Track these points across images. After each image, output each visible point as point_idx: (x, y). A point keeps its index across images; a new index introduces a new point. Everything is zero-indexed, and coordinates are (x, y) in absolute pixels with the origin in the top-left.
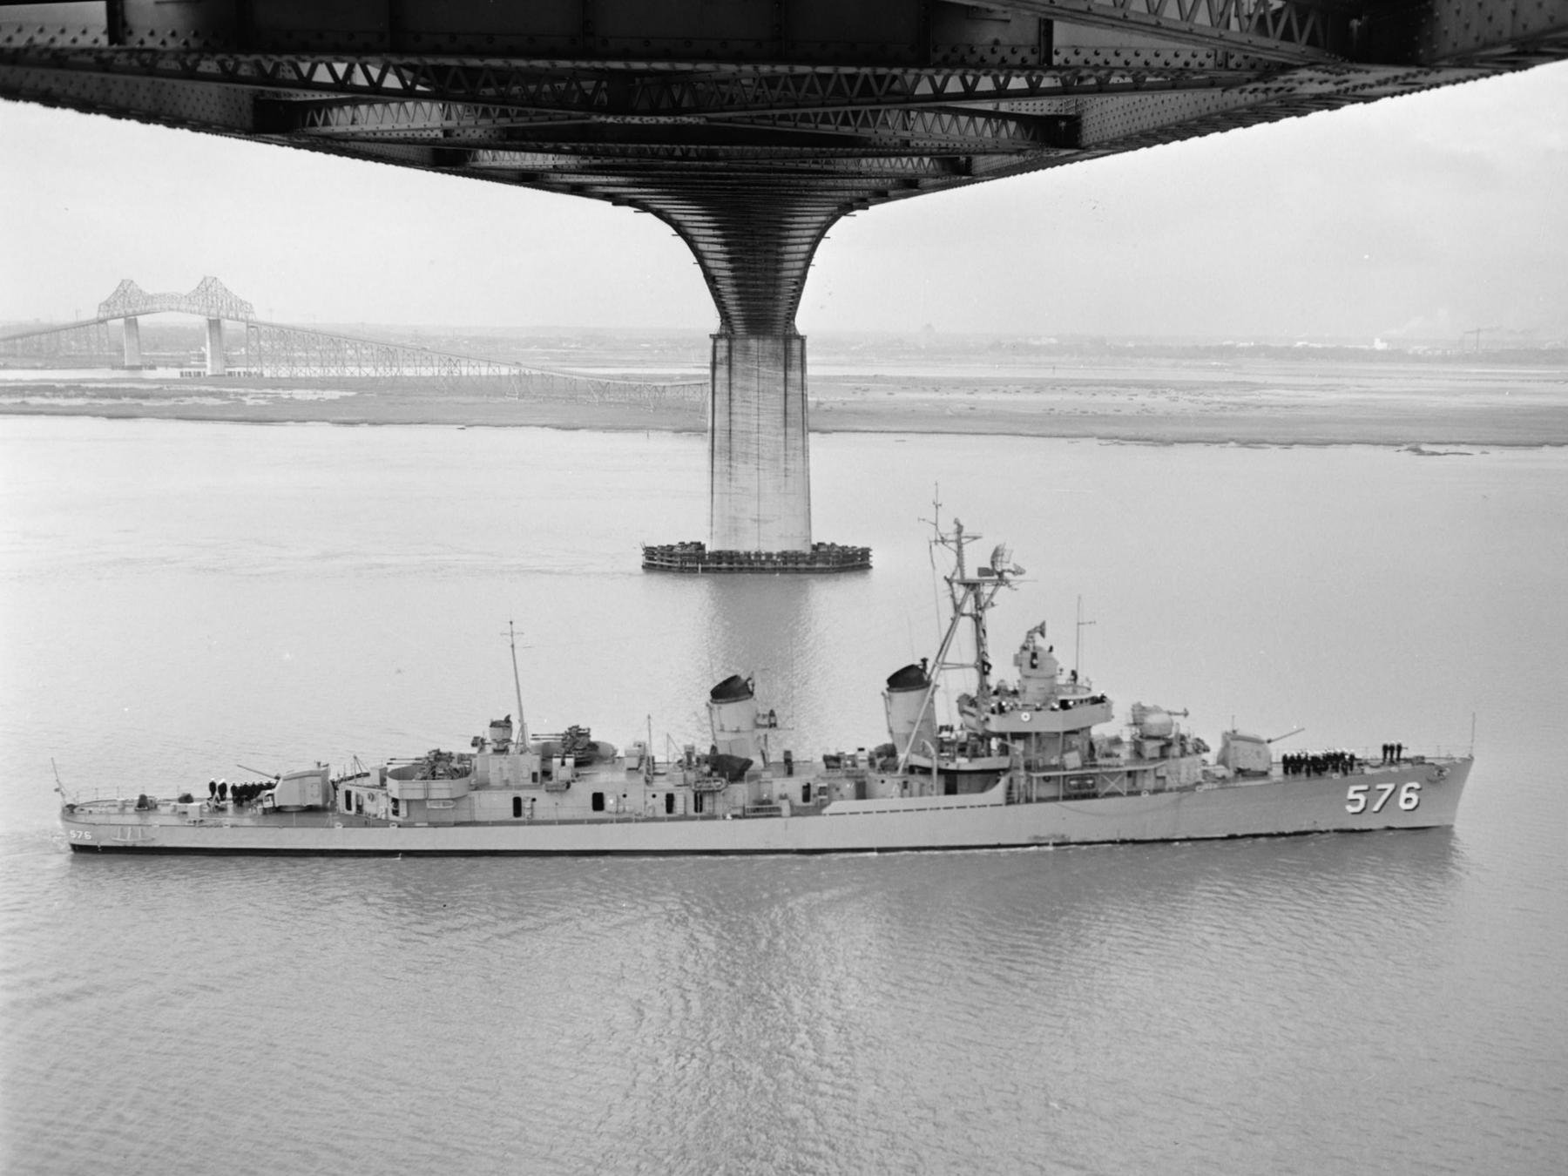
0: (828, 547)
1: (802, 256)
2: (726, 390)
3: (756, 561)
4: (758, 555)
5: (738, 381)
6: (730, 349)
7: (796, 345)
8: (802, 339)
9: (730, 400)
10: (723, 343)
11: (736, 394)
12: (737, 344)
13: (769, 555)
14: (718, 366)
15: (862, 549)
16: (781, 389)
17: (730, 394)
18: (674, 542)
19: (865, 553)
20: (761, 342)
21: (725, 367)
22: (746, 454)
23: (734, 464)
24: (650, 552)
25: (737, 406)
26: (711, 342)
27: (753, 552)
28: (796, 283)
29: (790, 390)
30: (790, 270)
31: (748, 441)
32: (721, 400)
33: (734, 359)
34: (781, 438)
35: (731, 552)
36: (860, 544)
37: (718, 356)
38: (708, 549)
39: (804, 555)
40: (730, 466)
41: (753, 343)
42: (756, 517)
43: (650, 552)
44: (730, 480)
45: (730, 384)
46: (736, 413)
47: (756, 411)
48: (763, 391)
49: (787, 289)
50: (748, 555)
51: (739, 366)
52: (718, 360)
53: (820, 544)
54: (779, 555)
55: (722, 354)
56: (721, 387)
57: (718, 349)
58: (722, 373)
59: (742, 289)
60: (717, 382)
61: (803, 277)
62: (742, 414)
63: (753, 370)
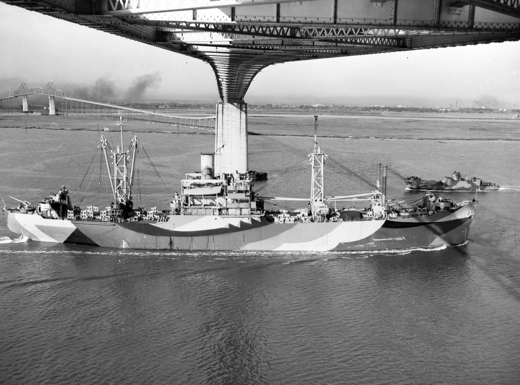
1: (250, 77)
8: (246, 104)
14: (219, 113)
19: (266, 174)
21: (221, 113)
25: (225, 126)
28: (246, 86)
30: (246, 82)
34: (239, 136)
36: (264, 172)
37: (219, 109)
42: (230, 162)
49: (244, 88)
52: (219, 111)
59: (229, 88)
61: (249, 84)
63: (230, 114)
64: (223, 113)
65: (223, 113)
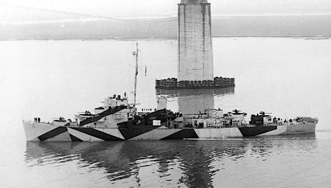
0: (220, 78)
2: (183, 23)
3: (195, 84)
4: (195, 82)
5: (188, 20)
6: (185, 8)
7: (207, 7)
9: (185, 26)
10: (182, 7)
11: (187, 24)
12: (187, 7)
13: (200, 82)
14: (180, 15)
15: (232, 79)
16: (202, 22)
17: (185, 25)
18: (166, 78)
20: (195, 6)
21: (183, 15)
22: (191, 46)
23: (186, 49)
24: (158, 82)
26: (177, 6)
27: (194, 81)
29: (205, 22)
31: (191, 41)
32: (182, 26)
33: (186, 12)
35: (186, 81)
37: (180, 11)
38: (178, 81)
39: (212, 81)
40: (185, 50)
41: (193, 6)
43: (158, 82)
44: (185, 55)
45: (185, 21)
46: (187, 31)
47: (194, 30)
48: (196, 23)
50: (192, 82)
51: (188, 15)
52: (180, 13)
53: (216, 77)
54: (203, 82)
55: (182, 11)
56: (182, 22)
57: (181, 9)
58: (182, 17)
60: (180, 21)
62: (189, 31)
63: (193, 16)
64: (185, 15)
65: (185, 15)
